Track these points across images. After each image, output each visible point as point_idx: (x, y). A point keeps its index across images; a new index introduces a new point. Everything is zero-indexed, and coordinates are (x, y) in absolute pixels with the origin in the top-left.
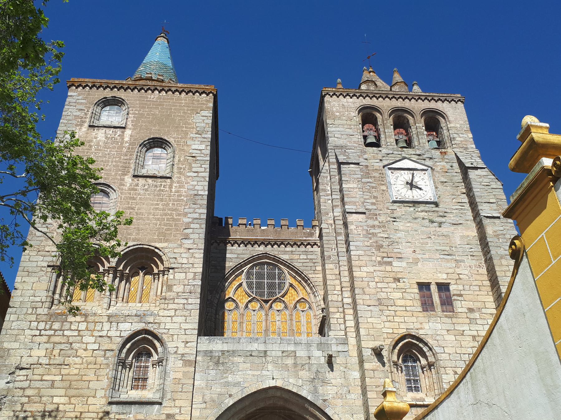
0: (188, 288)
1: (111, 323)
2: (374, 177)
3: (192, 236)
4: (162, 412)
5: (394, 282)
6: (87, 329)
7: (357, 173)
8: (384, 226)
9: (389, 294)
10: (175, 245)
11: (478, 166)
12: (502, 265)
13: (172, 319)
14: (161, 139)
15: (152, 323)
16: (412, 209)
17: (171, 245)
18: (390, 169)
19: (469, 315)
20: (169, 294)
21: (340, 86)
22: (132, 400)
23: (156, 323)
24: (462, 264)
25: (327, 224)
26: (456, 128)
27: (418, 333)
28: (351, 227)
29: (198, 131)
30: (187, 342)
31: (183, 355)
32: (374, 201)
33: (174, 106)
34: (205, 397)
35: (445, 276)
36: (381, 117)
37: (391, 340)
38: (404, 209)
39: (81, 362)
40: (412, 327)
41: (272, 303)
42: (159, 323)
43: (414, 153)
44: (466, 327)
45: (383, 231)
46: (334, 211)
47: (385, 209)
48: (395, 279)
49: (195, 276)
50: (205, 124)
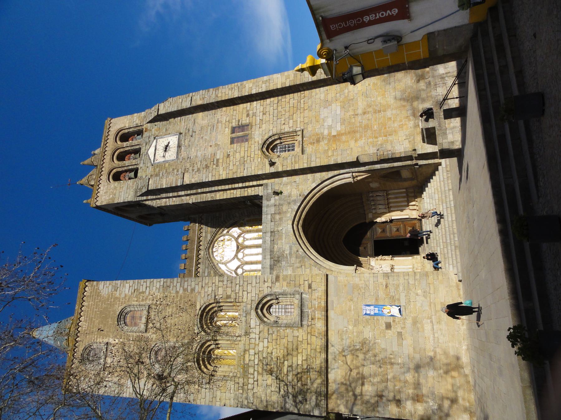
0: (229, 285)
2: (159, 171)
3: (193, 286)
4: (307, 292)
6: (254, 349)
8: (193, 164)
9: (237, 160)
10: (199, 296)
11: (157, 108)
12: (221, 97)
13: (249, 293)
14: (119, 315)
15: (251, 306)
16: (183, 148)
17: (199, 299)
20: (232, 297)
21: (89, 201)
22: (300, 312)
23: (251, 303)
24: (220, 119)
25: (189, 199)
27: (261, 144)
28: (193, 181)
29: (115, 290)
30: (264, 281)
31: (272, 283)
32: (176, 170)
33: (93, 308)
35: (227, 129)
37: (265, 159)
39: (275, 350)
40: (257, 147)
41: (239, 243)
42: (252, 301)
43: (144, 148)
44: (258, 118)
45: (196, 164)
47: (182, 163)
49: (221, 281)
50: (110, 286)
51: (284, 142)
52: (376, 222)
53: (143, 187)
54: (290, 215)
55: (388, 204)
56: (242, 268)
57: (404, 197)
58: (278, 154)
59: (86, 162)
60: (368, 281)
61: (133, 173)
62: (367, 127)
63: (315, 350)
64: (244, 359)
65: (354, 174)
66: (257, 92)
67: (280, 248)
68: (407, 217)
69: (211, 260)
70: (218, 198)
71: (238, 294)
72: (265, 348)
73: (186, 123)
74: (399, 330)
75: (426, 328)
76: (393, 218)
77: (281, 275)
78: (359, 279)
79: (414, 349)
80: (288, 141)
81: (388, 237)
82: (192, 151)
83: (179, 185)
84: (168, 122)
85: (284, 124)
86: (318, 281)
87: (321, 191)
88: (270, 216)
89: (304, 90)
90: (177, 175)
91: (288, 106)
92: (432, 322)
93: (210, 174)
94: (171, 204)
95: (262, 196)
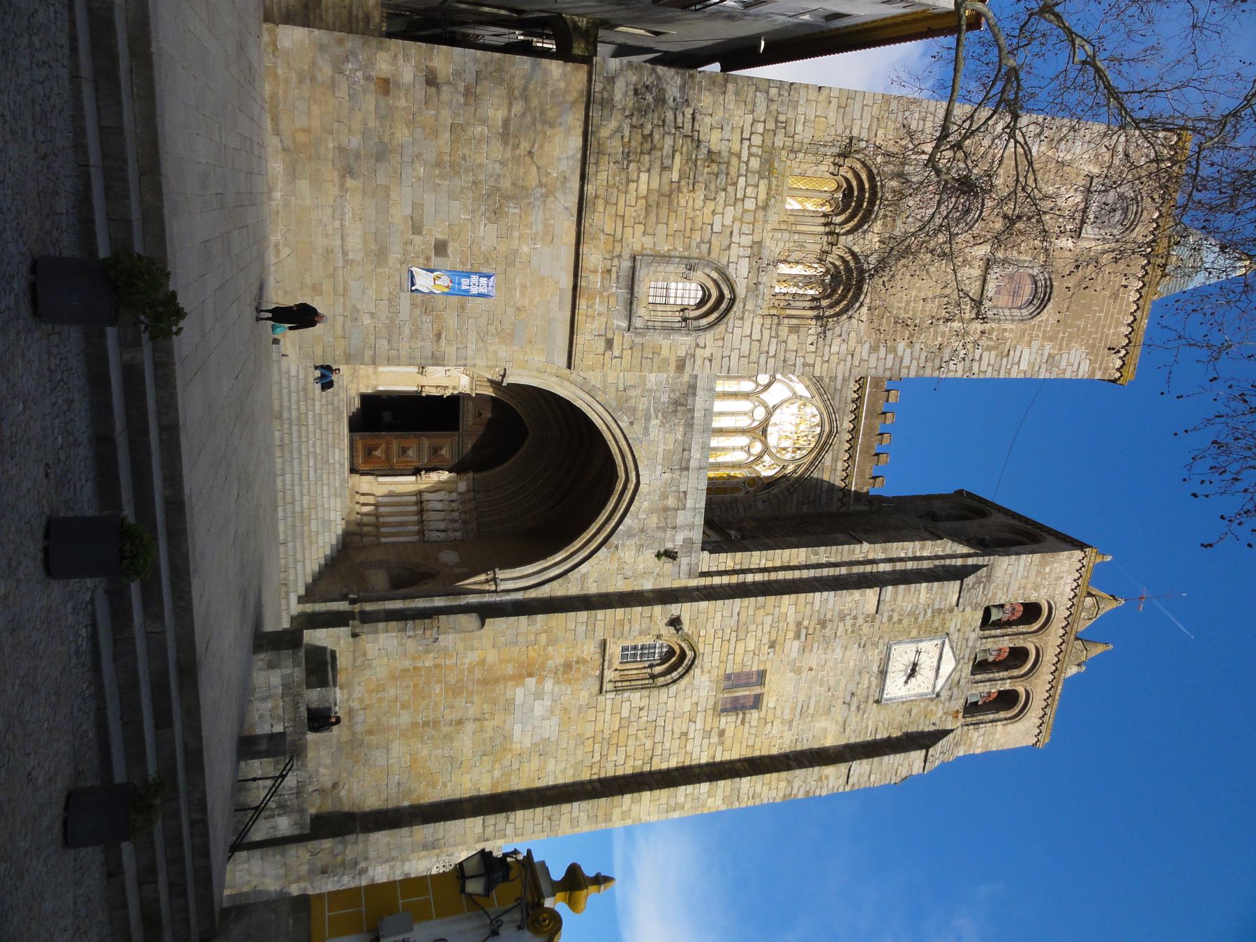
0: (791, 356)
1: (751, 247)
2: (933, 621)
3: (874, 356)
4: (616, 332)
5: (770, 641)
6: (745, 211)
8: (853, 632)
12: (779, 780)
16: (875, 669)
19: (715, 731)
21: (1099, 560)
24: (786, 728)
26: (994, 733)
28: (856, 594)
30: (710, 361)
32: (895, 619)
33: (1106, 316)
34: (632, 389)
35: (771, 705)
37: (690, 633)
38: (877, 658)
39: (697, 207)
40: (705, 660)
41: (761, 441)
42: (742, 319)
43: (964, 675)
44: (699, 725)
45: (846, 630)
48: (774, 642)
49: (809, 365)
51: (645, 668)
52: (450, 472)
53: (973, 587)
54: (642, 504)
55: (422, 522)
56: (758, 384)
57: (385, 525)
58: (658, 643)
59: (1099, 649)
60: (478, 350)
61: (994, 618)
62: (456, 690)
63: (607, 203)
64: (769, 189)
65: (493, 588)
66: (697, 785)
67: (670, 431)
68: (381, 479)
69: (826, 408)
70: (803, 551)
71: (773, 334)
72: (721, 211)
73: (864, 725)
74: (418, 239)
75: (359, 240)
76: (413, 478)
77: (672, 374)
78: (499, 355)
79: (388, 196)
80: (634, 670)
81: (427, 437)
82: (855, 660)
83: (890, 588)
84: (904, 730)
85: (641, 709)
86: (592, 356)
87: (568, 553)
88: (688, 506)
89: (591, 782)
90: (893, 610)
91: (631, 750)
92: (345, 253)
93: (817, 607)
94: (912, 544)
95: (703, 549)
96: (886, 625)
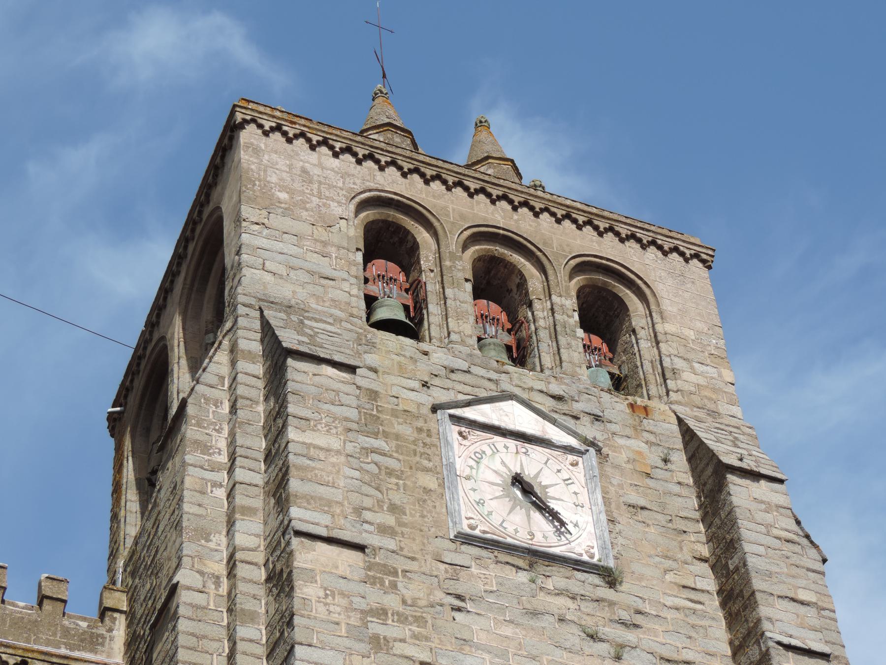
2: (397, 437)
7: (345, 399)
8: (420, 620)
11: (763, 471)
16: (523, 577)
18: (457, 420)
32: (390, 520)
36: (434, 246)
45: (415, 636)
46: (238, 525)
47: (429, 558)
94: (191, 470)
96: (405, 542)
